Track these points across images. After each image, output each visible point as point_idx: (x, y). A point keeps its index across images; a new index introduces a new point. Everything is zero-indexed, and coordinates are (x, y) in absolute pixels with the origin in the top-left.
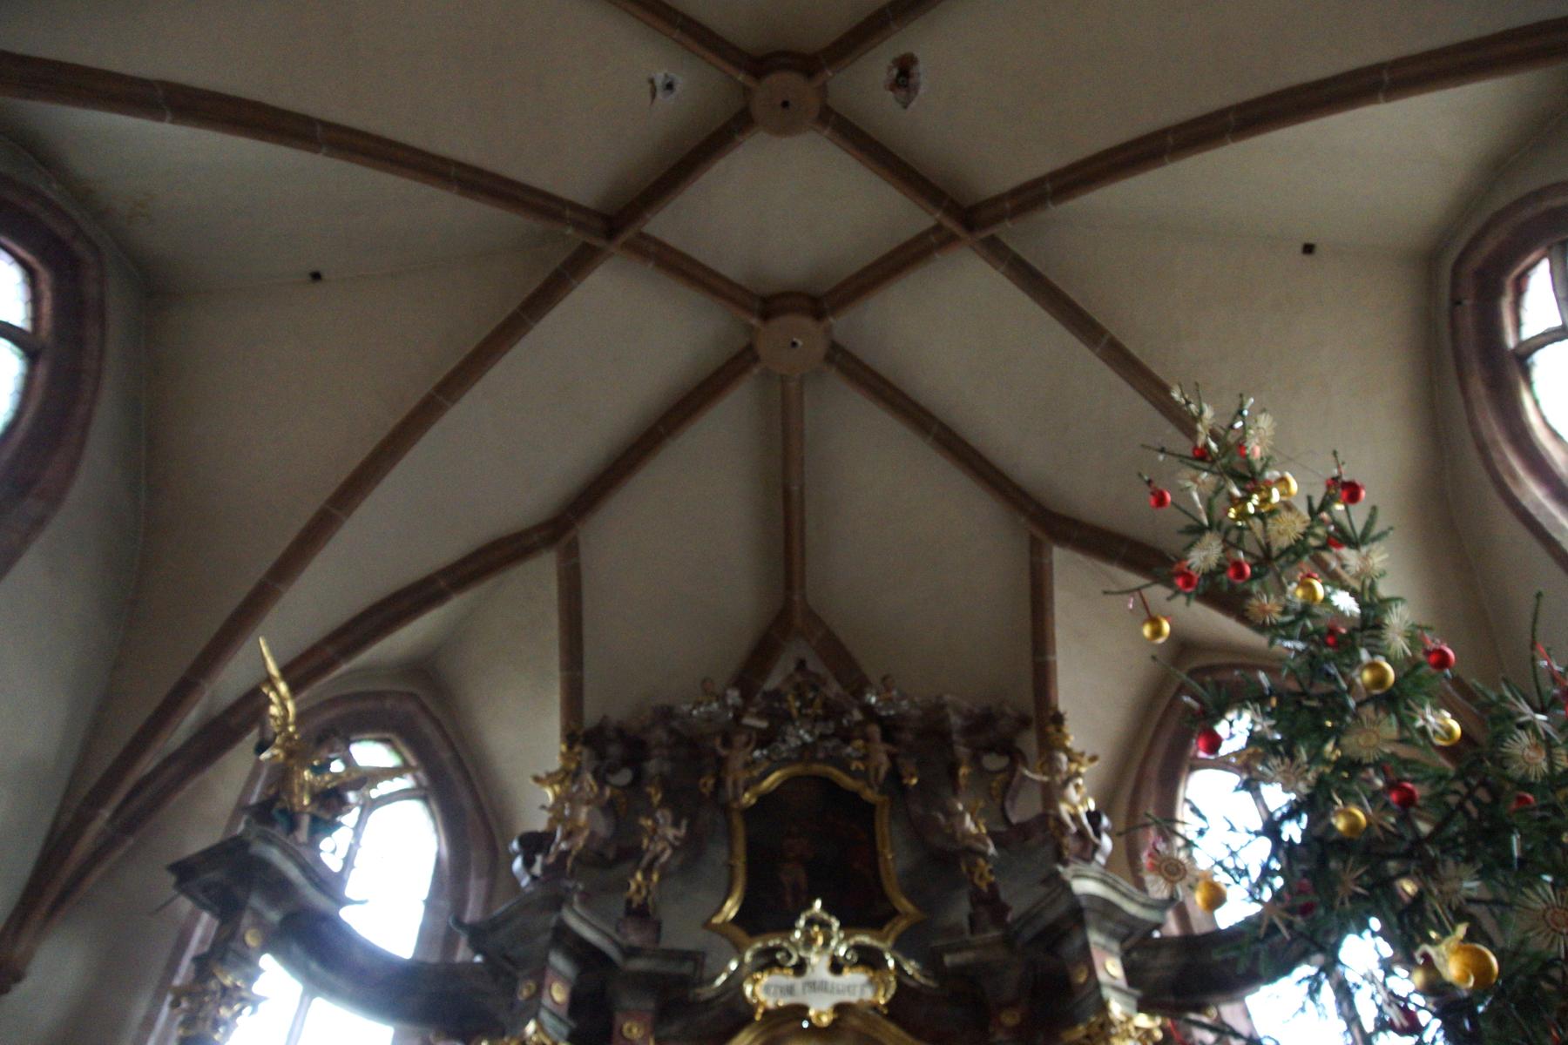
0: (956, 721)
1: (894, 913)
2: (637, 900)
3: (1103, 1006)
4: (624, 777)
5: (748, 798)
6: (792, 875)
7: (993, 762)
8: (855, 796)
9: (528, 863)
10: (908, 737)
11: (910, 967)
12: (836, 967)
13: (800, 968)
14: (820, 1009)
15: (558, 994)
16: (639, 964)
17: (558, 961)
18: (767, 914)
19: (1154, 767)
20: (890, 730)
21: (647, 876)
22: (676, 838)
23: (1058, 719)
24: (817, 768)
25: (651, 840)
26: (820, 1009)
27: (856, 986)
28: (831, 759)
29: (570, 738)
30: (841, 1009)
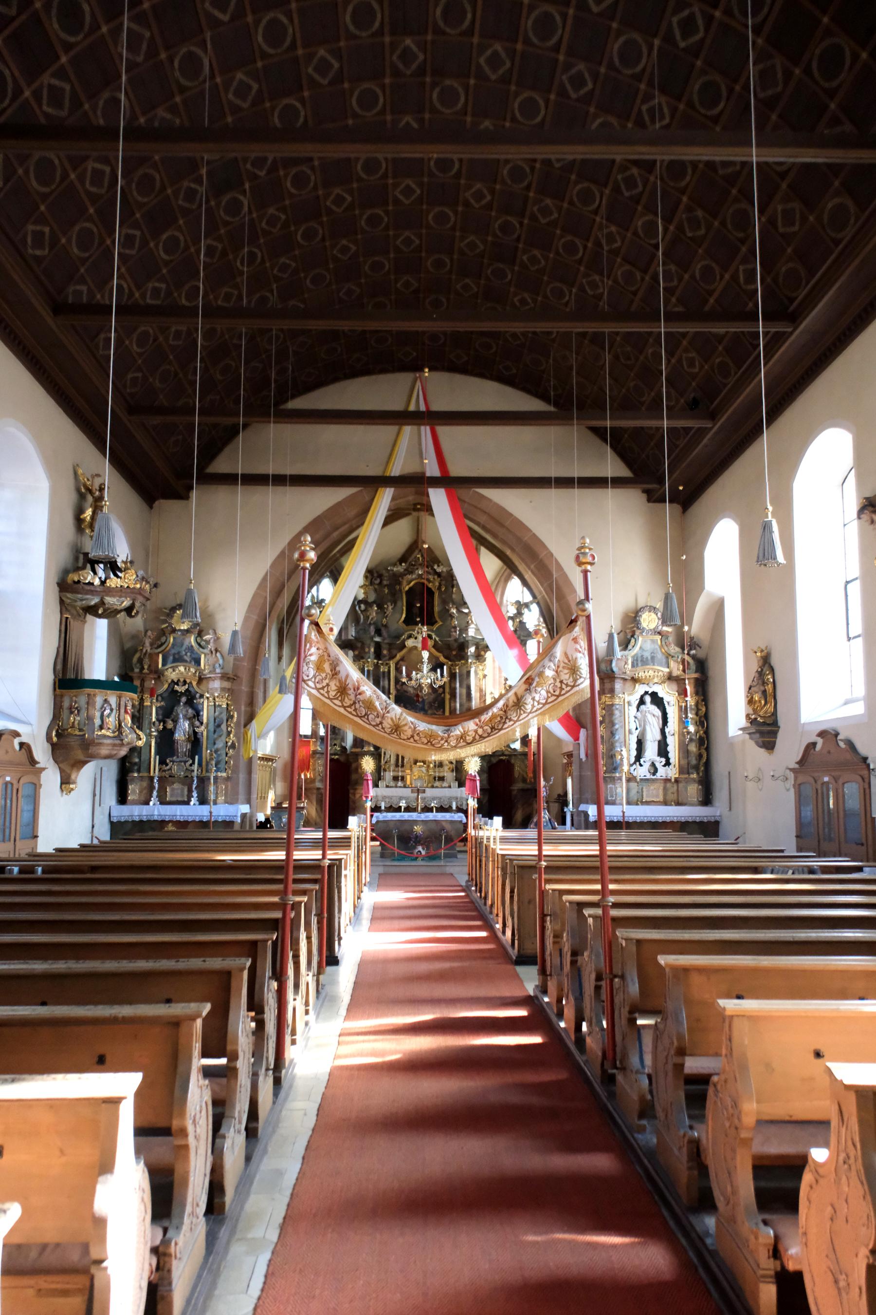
1: (436, 622)
4: (378, 581)
5: (407, 588)
9: (360, 607)
10: (443, 575)
11: (437, 639)
13: (416, 638)
15: (372, 650)
16: (386, 641)
17: (373, 644)
18: (410, 621)
20: (439, 575)
24: (422, 581)
29: (366, 577)
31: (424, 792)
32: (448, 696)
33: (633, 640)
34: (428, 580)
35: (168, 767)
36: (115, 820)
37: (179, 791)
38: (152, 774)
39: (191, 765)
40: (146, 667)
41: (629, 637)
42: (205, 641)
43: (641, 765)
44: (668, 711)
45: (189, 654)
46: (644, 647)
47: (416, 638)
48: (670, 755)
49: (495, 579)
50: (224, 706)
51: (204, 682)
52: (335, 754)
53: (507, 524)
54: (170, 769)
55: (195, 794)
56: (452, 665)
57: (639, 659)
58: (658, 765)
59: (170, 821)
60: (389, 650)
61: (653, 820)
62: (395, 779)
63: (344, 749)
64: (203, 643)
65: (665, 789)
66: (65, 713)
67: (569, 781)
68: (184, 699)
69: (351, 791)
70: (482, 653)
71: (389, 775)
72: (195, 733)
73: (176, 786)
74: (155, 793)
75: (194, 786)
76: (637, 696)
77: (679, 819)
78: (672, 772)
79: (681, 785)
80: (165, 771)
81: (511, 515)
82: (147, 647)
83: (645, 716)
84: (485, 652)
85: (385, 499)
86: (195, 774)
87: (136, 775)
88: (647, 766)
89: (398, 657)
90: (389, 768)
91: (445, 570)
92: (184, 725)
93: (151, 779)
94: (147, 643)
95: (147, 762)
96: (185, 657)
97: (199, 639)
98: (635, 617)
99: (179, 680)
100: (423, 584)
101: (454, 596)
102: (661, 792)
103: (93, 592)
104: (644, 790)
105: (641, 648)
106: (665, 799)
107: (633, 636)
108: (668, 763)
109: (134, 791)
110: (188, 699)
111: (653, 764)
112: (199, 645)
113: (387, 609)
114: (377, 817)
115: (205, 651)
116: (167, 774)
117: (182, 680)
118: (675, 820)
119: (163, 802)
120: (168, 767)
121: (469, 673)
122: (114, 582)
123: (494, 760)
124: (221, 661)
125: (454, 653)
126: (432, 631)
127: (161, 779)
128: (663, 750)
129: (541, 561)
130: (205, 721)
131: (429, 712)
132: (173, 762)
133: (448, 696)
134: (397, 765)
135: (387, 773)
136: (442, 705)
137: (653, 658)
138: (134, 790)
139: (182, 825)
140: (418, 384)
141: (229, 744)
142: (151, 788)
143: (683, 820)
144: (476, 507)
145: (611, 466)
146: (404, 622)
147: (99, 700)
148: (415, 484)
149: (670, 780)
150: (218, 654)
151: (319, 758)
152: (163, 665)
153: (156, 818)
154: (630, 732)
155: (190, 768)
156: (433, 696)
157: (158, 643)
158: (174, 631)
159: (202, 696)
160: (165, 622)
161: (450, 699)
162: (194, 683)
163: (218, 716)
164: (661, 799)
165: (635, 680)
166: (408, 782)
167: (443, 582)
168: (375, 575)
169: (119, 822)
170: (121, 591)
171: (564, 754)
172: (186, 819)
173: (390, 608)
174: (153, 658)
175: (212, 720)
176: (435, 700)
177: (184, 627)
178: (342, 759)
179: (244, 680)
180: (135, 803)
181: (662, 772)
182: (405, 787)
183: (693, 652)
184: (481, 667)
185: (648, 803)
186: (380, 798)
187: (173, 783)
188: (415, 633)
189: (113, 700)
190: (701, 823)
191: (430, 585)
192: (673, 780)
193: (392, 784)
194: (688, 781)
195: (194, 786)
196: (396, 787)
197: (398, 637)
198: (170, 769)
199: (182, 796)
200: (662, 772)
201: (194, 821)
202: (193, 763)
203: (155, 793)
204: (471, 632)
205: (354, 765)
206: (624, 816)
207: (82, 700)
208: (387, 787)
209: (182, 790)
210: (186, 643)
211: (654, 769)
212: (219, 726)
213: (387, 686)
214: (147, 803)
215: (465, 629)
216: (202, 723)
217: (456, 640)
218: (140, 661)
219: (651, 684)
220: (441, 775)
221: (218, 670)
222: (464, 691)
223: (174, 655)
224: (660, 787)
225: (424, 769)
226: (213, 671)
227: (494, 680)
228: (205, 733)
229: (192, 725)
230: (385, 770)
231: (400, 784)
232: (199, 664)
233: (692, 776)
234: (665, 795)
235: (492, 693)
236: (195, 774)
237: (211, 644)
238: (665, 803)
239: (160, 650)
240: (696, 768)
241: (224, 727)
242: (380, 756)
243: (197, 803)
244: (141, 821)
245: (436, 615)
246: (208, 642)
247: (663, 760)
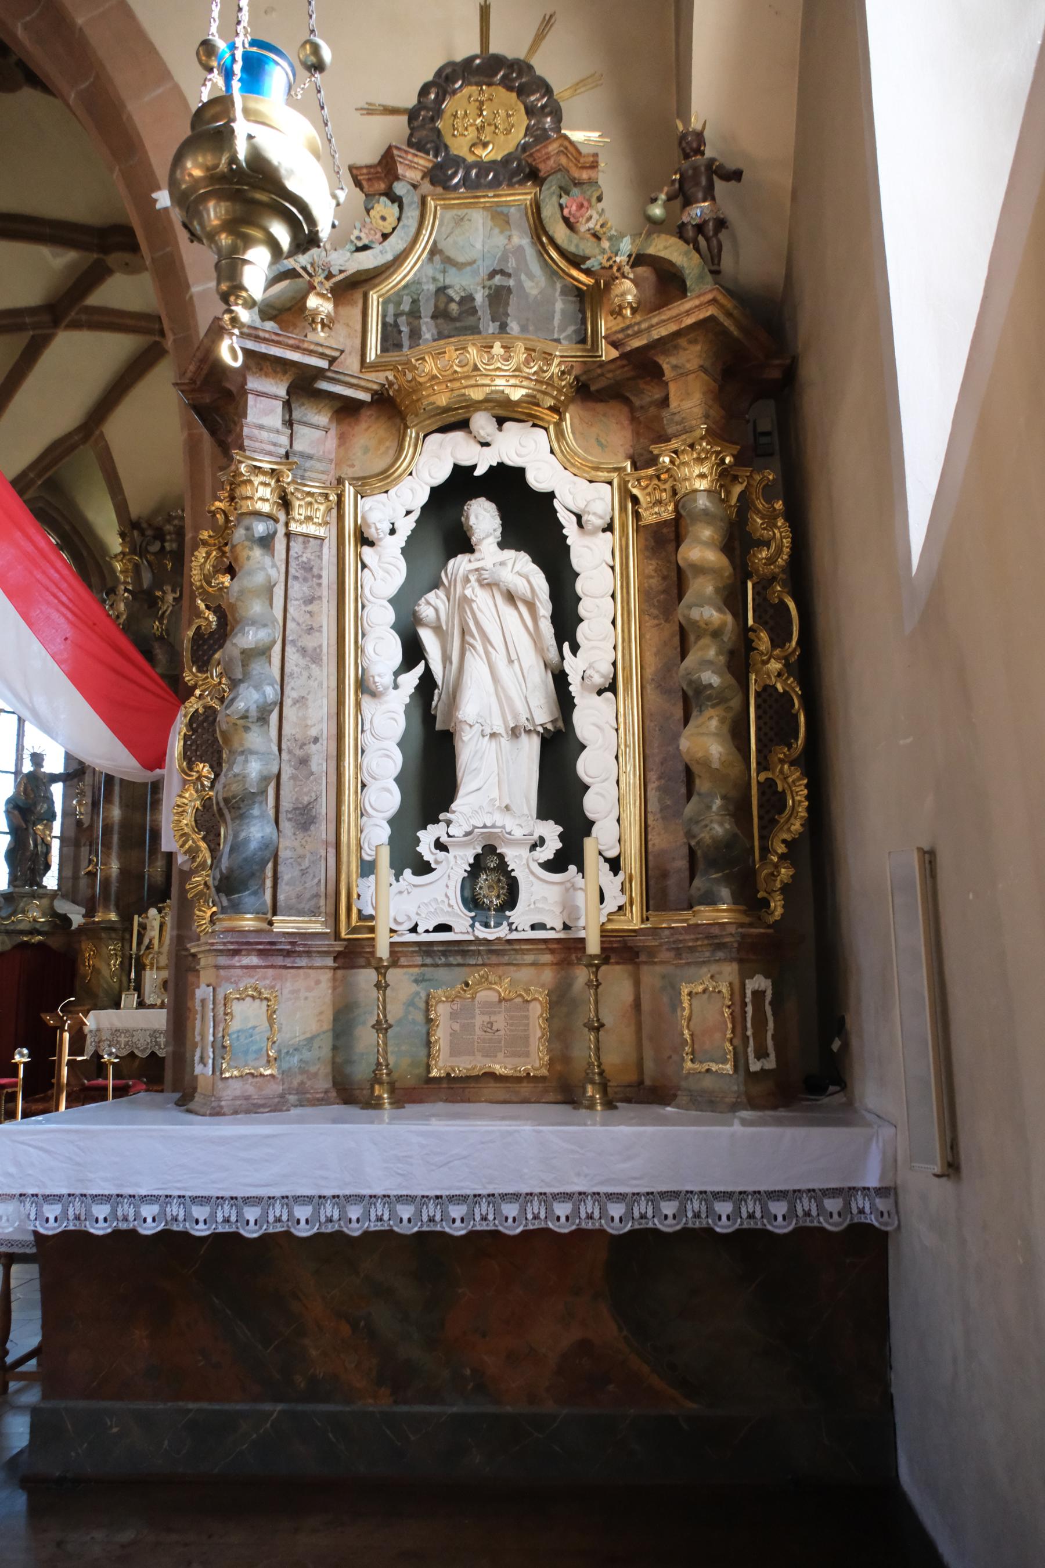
2: (158, 633)
4: (155, 547)
21: (161, 623)
22: (174, 599)
25: (162, 602)
43: (423, 868)
44: (577, 560)
46: (448, 247)
48: (593, 804)
57: (427, 310)
61: (406, 1220)
65: (560, 1001)
76: (412, 493)
83: (465, 601)
88: (453, 868)
104: (442, 1012)
105: (434, 251)
108: (567, 858)
113: (163, 599)
118: (562, 1218)
128: (560, 791)
137: (499, 298)
143: (617, 1220)
164: (535, 1059)
165: (392, 408)
168: (149, 532)
173: (170, 598)
178: (56, 943)
181: (542, 901)
183: (700, 210)
185: (458, 1090)
186: (105, 1035)
190: (750, 1242)
200: (542, 901)
208: (141, 1005)
211: (490, 880)
219: (482, 423)
234: (559, 1035)
238: (562, 1089)
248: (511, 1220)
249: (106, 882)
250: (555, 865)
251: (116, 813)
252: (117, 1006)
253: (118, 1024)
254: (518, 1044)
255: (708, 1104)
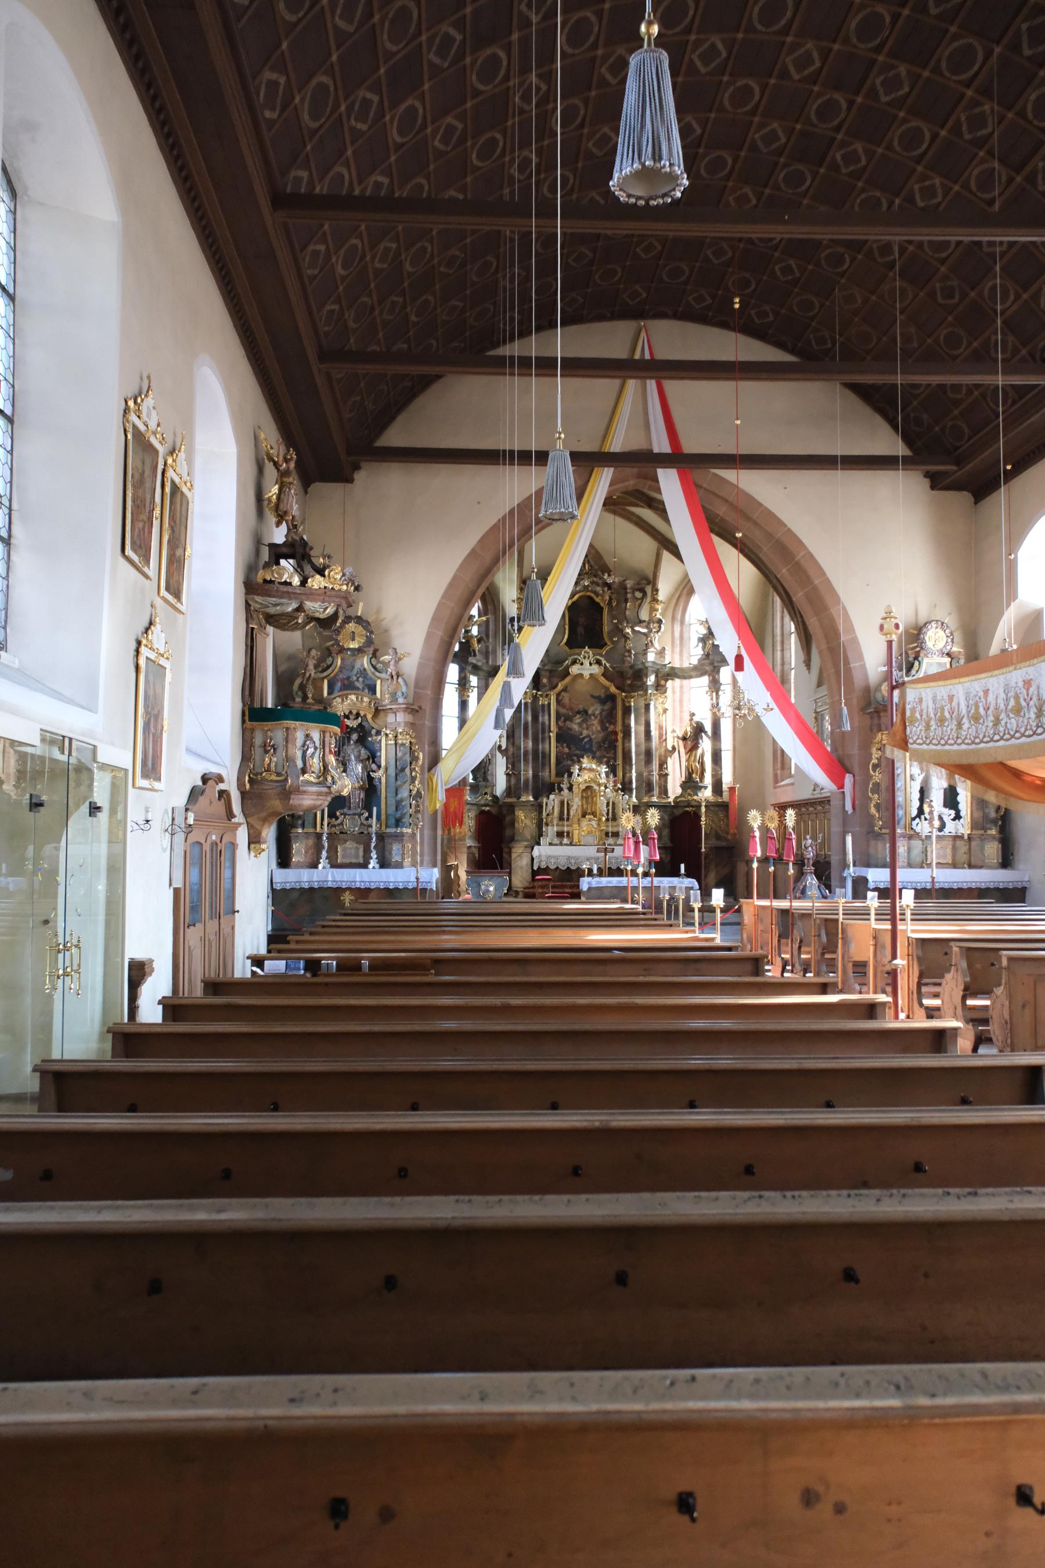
0: (629, 586)
3: (646, 690)
6: (580, 630)
7: (639, 595)
8: (598, 604)
10: (615, 586)
12: (591, 664)
13: (582, 664)
14: (586, 674)
16: (546, 668)
19: (685, 591)
20: (609, 586)
23: (657, 590)
24: (589, 594)
26: (586, 674)
27: (596, 669)
28: (592, 591)
30: (591, 675)
31: (613, 851)
32: (620, 736)
33: (916, 663)
34: (597, 594)
35: (339, 821)
36: (278, 887)
37: (353, 851)
38: (318, 829)
39: (367, 819)
40: (310, 696)
41: (911, 659)
42: (383, 663)
45: (361, 679)
47: (582, 664)
48: (961, 806)
49: (677, 590)
50: (408, 744)
51: (382, 714)
52: (486, 805)
53: (754, 517)
54: (342, 824)
55: (374, 855)
56: (626, 697)
58: (946, 819)
59: (349, 889)
60: (549, 678)
61: (946, 886)
62: (560, 834)
63: (495, 797)
64: (379, 666)
65: (954, 849)
66: (258, 752)
67: (849, 839)
68: (355, 736)
69: (505, 850)
70: (663, 682)
71: (551, 831)
72: (370, 779)
73: (349, 844)
74: (324, 854)
75: (373, 845)
77: (979, 885)
78: (963, 827)
79: (973, 843)
80: (334, 826)
81: (761, 505)
82: (311, 671)
84: (666, 681)
85: (603, 481)
86: (374, 829)
87: (300, 830)
89: (560, 687)
90: (552, 821)
91: (616, 580)
92: (357, 769)
93: (319, 836)
94: (311, 664)
95: (312, 816)
96: (357, 684)
97: (374, 661)
98: (919, 634)
99: (351, 712)
100: (590, 597)
101: (627, 613)
102: (949, 851)
103: (290, 595)
106: (954, 860)
107: (916, 658)
108: (958, 817)
109: (299, 851)
110: (359, 736)
111: (940, 818)
112: (374, 667)
114: (589, 883)
115: (383, 675)
116: (337, 830)
117: (354, 712)
118: (973, 886)
119: (334, 865)
120: (339, 821)
121: (647, 707)
122: (316, 582)
123: (678, 812)
124: (404, 689)
125: (629, 682)
126: (601, 655)
127: (330, 836)
129: (797, 563)
130: (383, 764)
131: (598, 754)
132: (345, 815)
133: (620, 736)
134: (561, 818)
135: (549, 828)
136: (613, 747)
138: (299, 850)
139: (363, 893)
140: (643, 334)
141: (414, 792)
142: (319, 847)
143: (983, 886)
144: (714, 494)
145: (887, 442)
146: (566, 644)
147: (300, 736)
148: (644, 461)
149: (961, 837)
150: (400, 680)
151: (469, 810)
152: (329, 693)
153: (330, 885)
154: (912, 778)
155: (365, 822)
156: (601, 735)
157: (322, 666)
158: (342, 650)
159: (378, 733)
160: (330, 638)
161: (624, 738)
162: (369, 717)
163: (401, 758)
166: (576, 840)
167: (614, 596)
169: (284, 890)
170: (325, 593)
171: (774, 806)
172: (367, 885)
174: (317, 684)
175: (393, 762)
176: (604, 740)
177: (354, 645)
178: (494, 811)
179: (428, 713)
180: (299, 866)
181: (951, 827)
182: (571, 844)
184: (661, 700)
186: (543, 859)
187: (345, 841)
188: (581, 658)
189: (316, 736)
191: (597, 600)
192: (966, 837)
193: (556, 841)
194: (983, 839)
195: (373, 845)
196: (561, 844)
197: (560, 662)
198: (342, 824)
199: (357, 857)
200: (951, 827)
201: (378, 889)
202: (370, 816)
203: (324, 854)
204: (651, 657)
205: (508, 819)
206: (933, 882)
207: (278, 736)
208: (551, 844)
209: (357, 849)
210: (358, 665)
212: (403, 770)
213: (547, 723)
214: (314, 865)
215: (645, 653)
216: (379, 767)
217: (632, 667)
218: (302, 687)
220: (615, 830)
221: (401, 700)
222: (642, 728)
223: (343, 680)
224: (949, 844)
225: (594, 823)
226: (394, 699)
227: (674, 715)
228: (383, 780)
229: (364, 768)
230: (547, 825)
231: (565, 841)
232: (374, 692)
233: (989, 832)
234: (954, 855)
235: (674, 731)
236: (374, 829)
237: (392, 667)
238: (954, 865)
239: (325, 674)
240: (994, 822)
241: (407, 770)
242: (541, 806)
243: (377, 866)
244: (311, 889)
245: (605, 636)
246: (386, 665)
247: (953, 812)
248: (965, 886)
249: (526, 781)
250: (954, 820)
251: (530, 744)
252: (539, 844)
253: (550, 853)
254: (945, 857)
255: (990, 867)
